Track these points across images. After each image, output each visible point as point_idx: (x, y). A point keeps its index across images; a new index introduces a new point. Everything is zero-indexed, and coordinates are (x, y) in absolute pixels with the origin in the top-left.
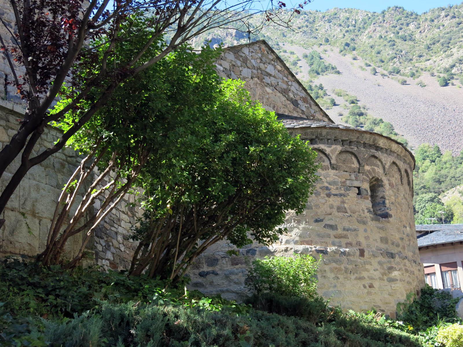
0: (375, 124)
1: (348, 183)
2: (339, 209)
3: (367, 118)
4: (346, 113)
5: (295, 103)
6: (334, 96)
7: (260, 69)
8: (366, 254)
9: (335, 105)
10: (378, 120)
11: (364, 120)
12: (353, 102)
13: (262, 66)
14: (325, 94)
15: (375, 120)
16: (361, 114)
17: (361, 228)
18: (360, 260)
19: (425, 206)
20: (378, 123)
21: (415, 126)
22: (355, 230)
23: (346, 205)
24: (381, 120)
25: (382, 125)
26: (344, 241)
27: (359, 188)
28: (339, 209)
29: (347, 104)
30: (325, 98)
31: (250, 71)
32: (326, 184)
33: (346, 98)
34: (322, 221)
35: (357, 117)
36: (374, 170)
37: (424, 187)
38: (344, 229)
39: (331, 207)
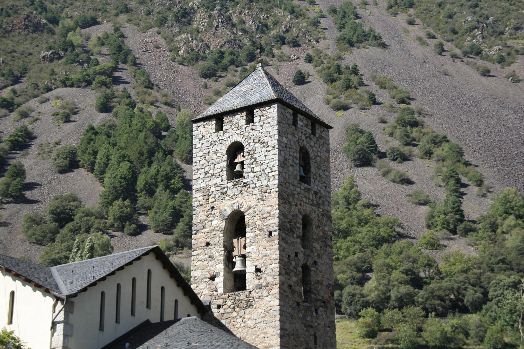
0: (435, 143)
3: (424, 130)
4: (392, 119)
6: (374, 88)
9: (375, 102)
10: (441, 137)
11: (417, 134)
12: (403, 101)
14: (361, 84)
15: (436, 137)
16: (415, 124)
19: (503, 293)
20: (441, 142)
21: (496, 151)
24: (445, 137)
25: (446, 146)
29: (394, 102)
30: (361, 89)
33: (394, 92)
35: (408, 128)
37: (503, 261)
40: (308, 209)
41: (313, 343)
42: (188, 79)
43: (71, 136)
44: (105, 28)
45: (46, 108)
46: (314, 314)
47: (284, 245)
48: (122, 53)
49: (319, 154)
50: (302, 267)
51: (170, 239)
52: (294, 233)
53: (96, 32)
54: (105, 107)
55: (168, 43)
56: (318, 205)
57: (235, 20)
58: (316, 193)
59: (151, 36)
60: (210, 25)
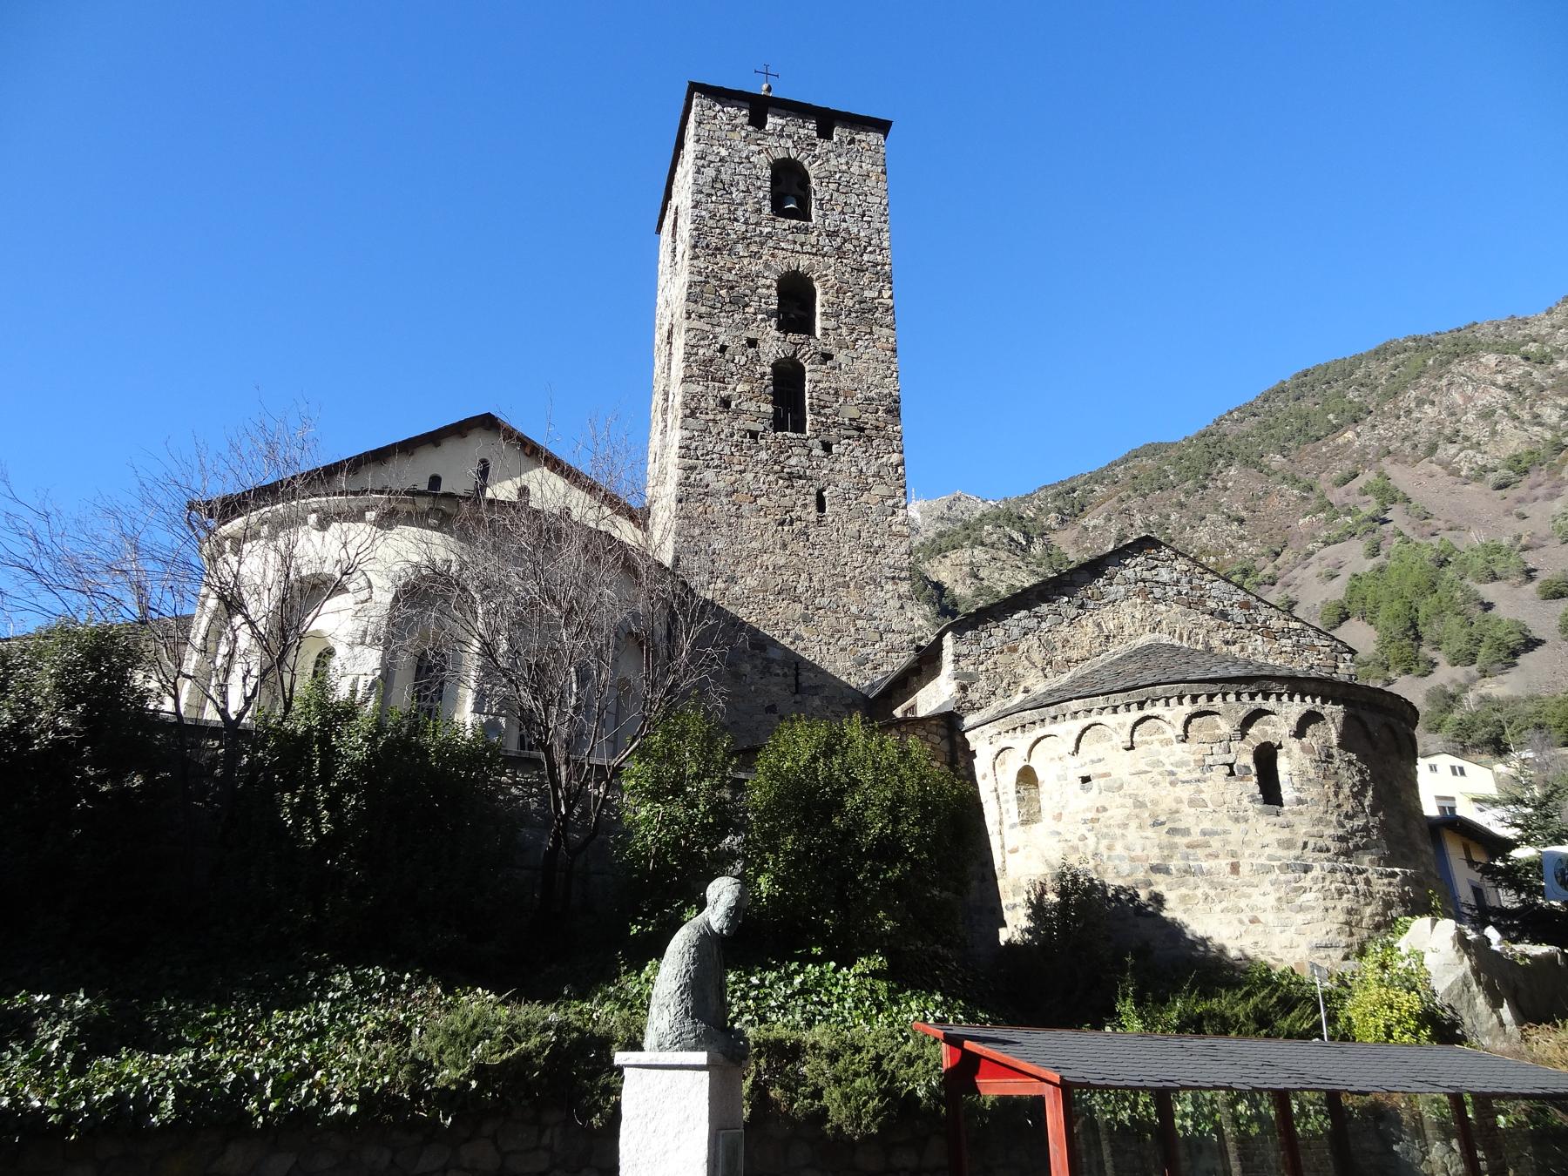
1: (1209, 760)
2: (1192, 803)
5: (1224, 615)
7: (1144, 581)
8: (1244, 869)
13: (1147, 575)
17: (1236, 831)
18: (1232, 879)
22: (1225, 832)
23: (1203, 796)
26: (1200, 852)
27: (1231, 766)
28: (1192, 803)
31: (1122, 589)
32: (1170, 768)
34: (1163, 823)
36: (1265, 733)
38: (1204, 833)
39: (1179, 801)
40: (804, 262)
41: (813, 508)
42: (1478, 496)
43: (1337, 590)
44: (1368, 477)
45: (1312, 570)
46: (818, 452)
47: (708, 328)
48: (1388, 495)
49: (844, 167)
50: (773, 366)
51: (1473, 670)
52: (747, 305)
53: (1356, 484)
54: (1375, 551)
55: (1445, 468)
56: (840, 253)
57: (1527, 417)
58: (832, 235)
59: (1425, 466)
60: (1494, 433)
